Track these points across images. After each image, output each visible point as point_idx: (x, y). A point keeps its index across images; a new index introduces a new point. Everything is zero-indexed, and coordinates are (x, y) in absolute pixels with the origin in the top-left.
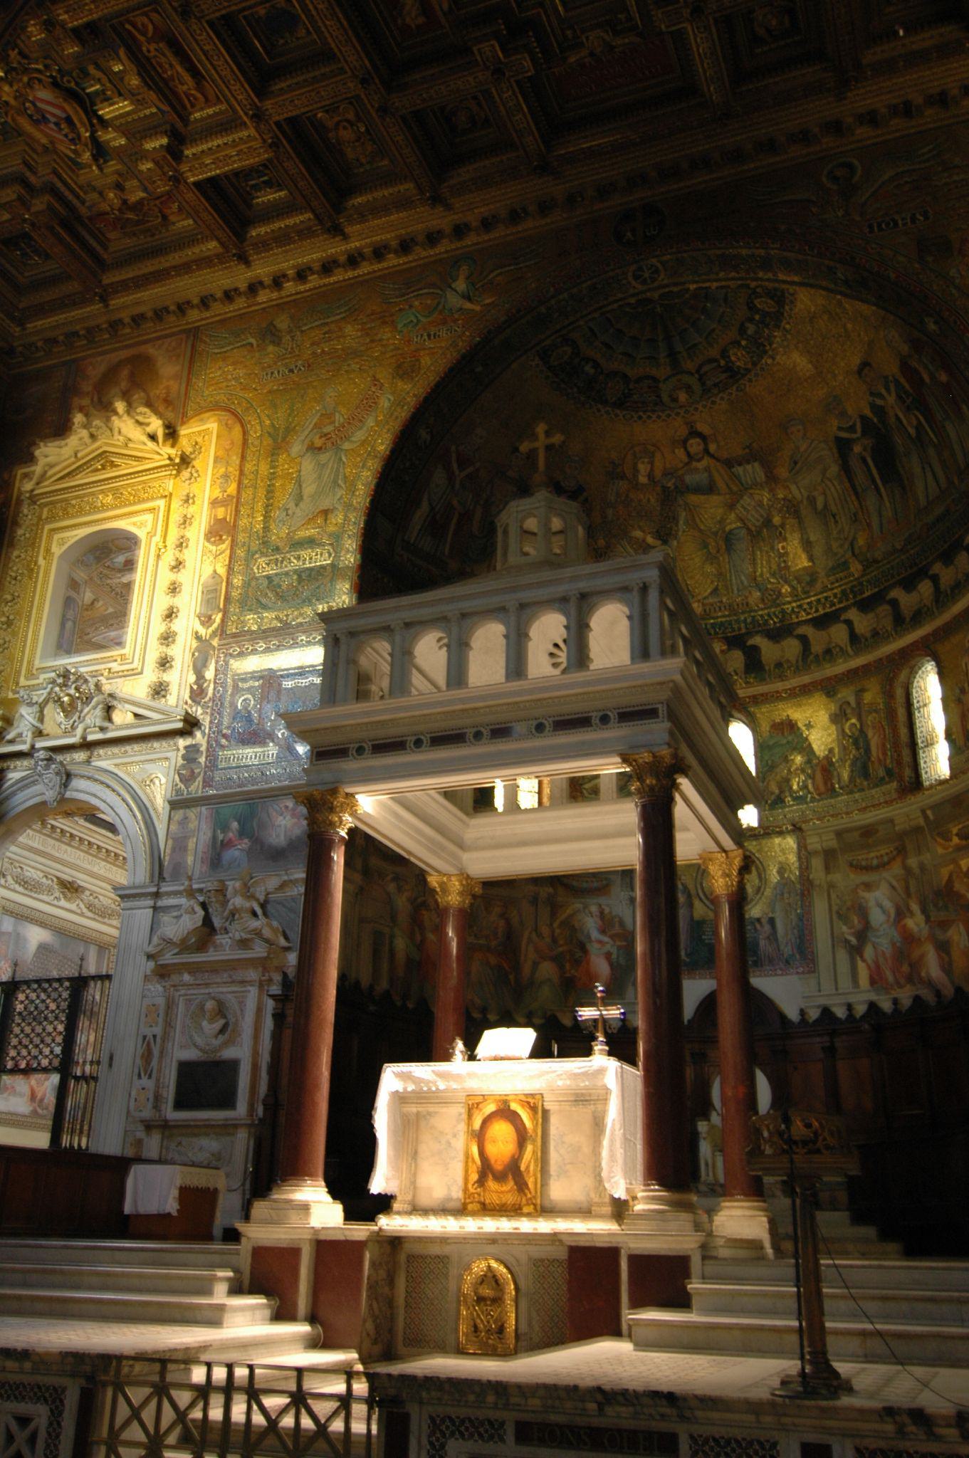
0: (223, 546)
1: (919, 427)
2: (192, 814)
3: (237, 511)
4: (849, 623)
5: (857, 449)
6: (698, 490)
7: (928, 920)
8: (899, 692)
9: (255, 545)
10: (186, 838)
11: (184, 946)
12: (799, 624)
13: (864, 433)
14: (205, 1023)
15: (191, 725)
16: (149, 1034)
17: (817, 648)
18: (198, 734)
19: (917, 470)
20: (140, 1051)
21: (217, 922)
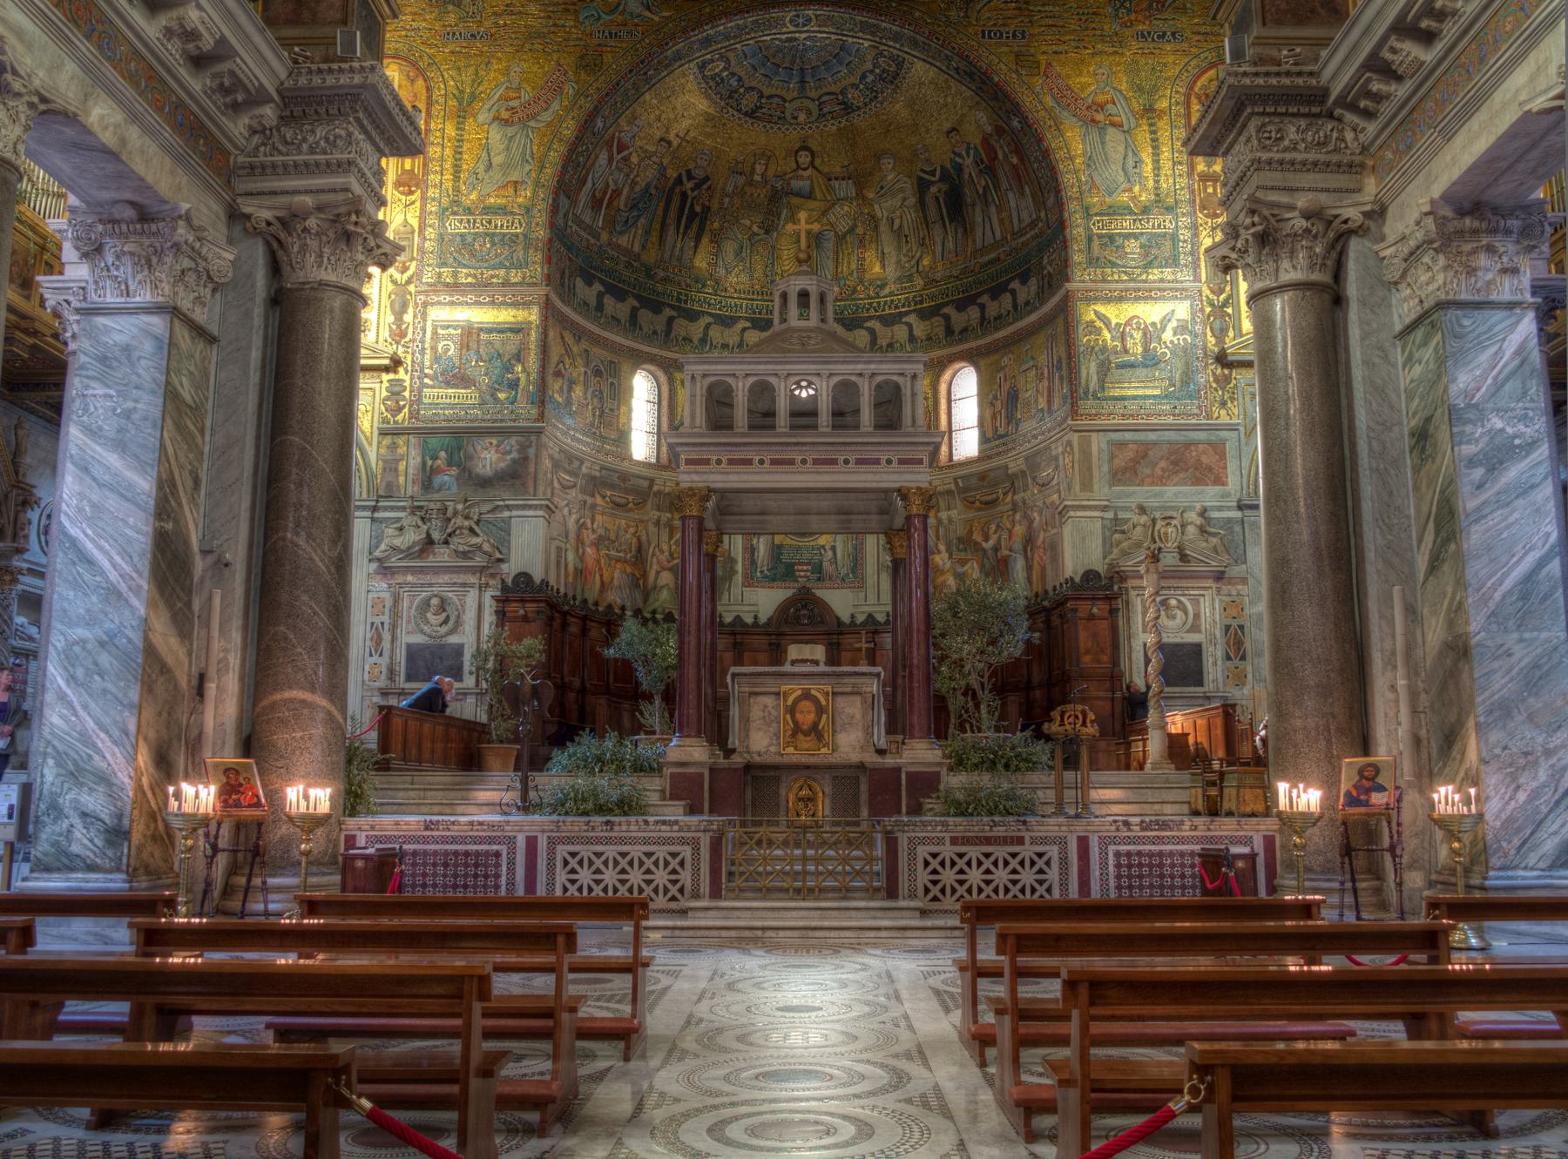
0: (413, 198)
1: (986, 188)
2: (401, 441)
3: (425, 165)
4: (910, 326)
5: (934, 189)
6: (798, 194)
7: (950, 557)
8: (943, 388)
9: (445, 201)
10: (397, 461)
11: (408, 553)
12: (870, 318)
13: (941, 180)
14: (429, 615)
15: (396, 363)
16: (377, 620)
17: (883, 342)
18: (401, 370)
19: (979, 219)
20: (369, 635)
21: (436, 536)
